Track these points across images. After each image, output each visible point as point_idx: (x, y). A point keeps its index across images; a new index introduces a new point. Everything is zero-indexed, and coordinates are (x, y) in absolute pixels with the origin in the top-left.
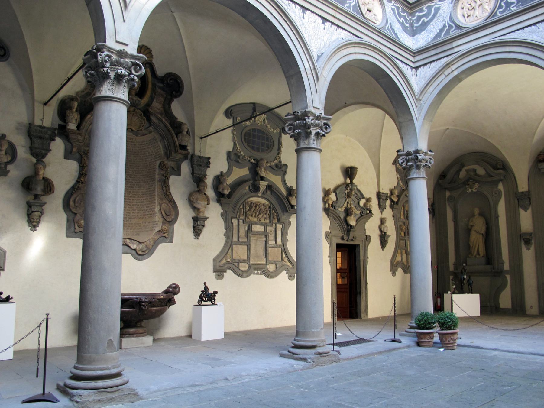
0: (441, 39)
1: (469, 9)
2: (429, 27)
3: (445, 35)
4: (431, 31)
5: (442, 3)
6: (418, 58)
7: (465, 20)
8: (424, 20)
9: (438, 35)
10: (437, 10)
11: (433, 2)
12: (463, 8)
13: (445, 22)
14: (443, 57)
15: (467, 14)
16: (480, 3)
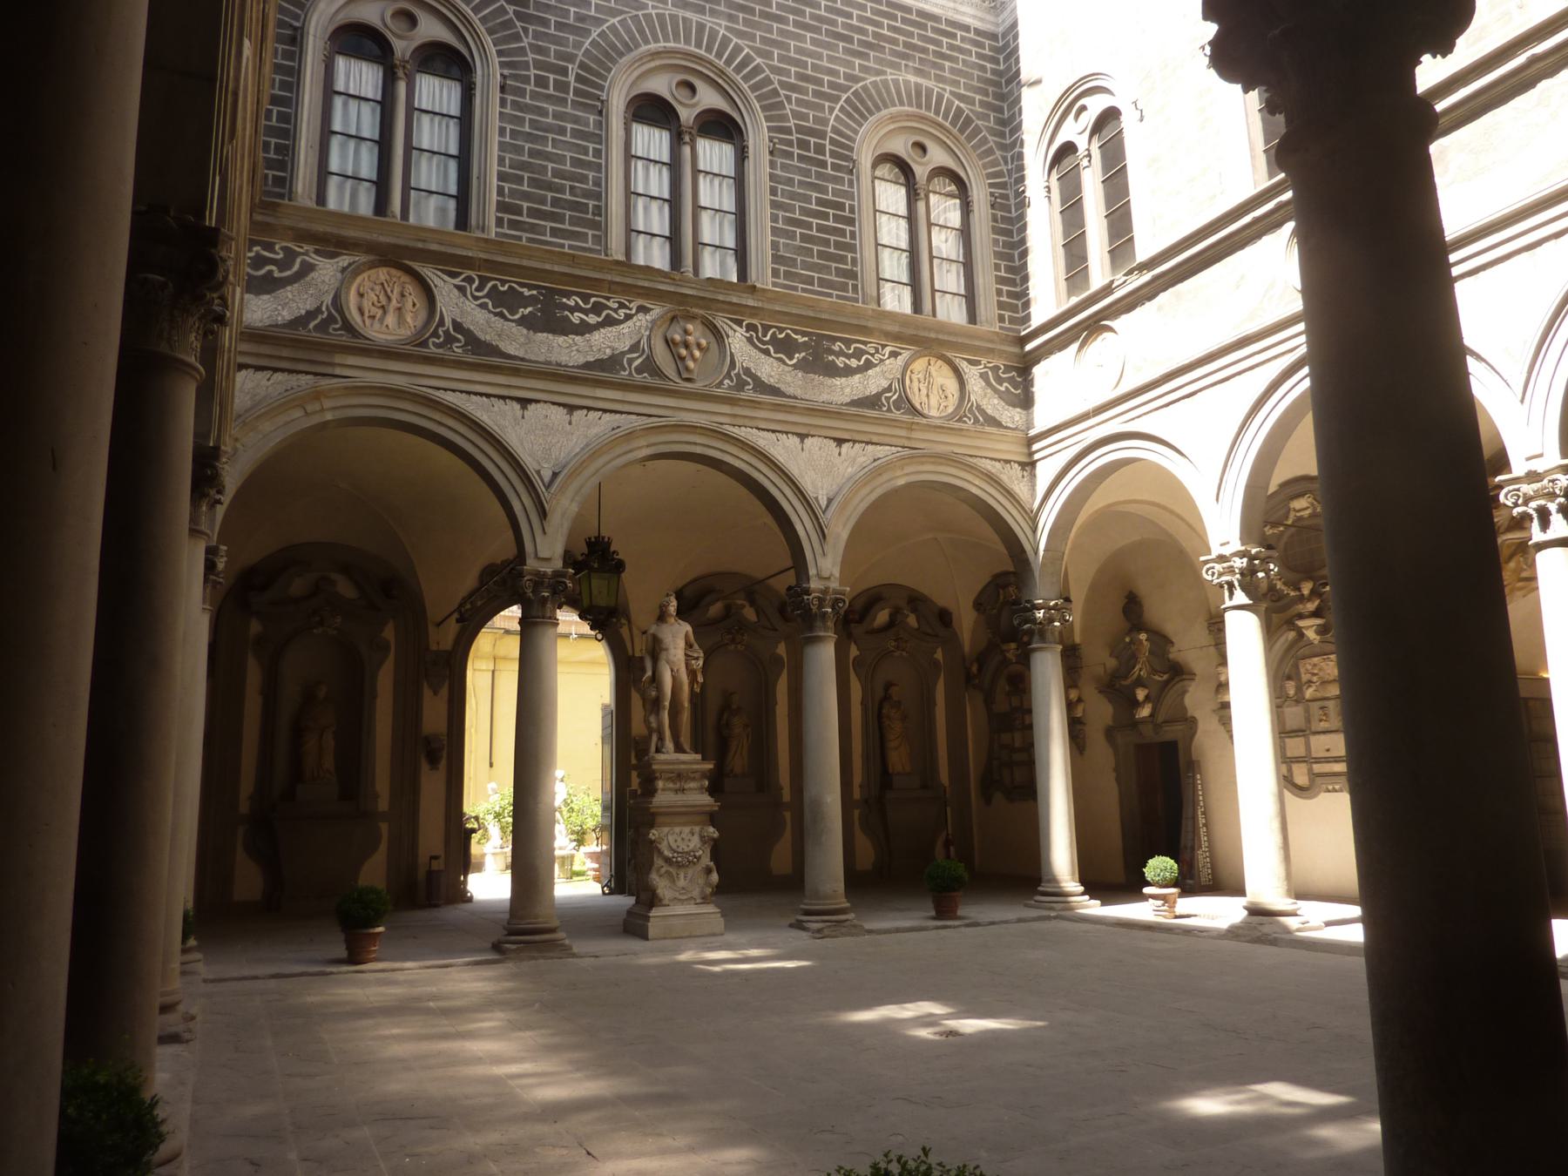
0: (303, 332)
1: (373, 304)
2: (281, 293)
3: (316, 327)
4: (286, 304)
5: (321, 259)
7: (364, 321)
8: (270, 272)
9: (300, 322)
10: (308, 268)
11: (302, 247)
12: (362, 295)
13: (322, 302)
14: (307, 373)
15: (369, 312)
16: (399, 305)
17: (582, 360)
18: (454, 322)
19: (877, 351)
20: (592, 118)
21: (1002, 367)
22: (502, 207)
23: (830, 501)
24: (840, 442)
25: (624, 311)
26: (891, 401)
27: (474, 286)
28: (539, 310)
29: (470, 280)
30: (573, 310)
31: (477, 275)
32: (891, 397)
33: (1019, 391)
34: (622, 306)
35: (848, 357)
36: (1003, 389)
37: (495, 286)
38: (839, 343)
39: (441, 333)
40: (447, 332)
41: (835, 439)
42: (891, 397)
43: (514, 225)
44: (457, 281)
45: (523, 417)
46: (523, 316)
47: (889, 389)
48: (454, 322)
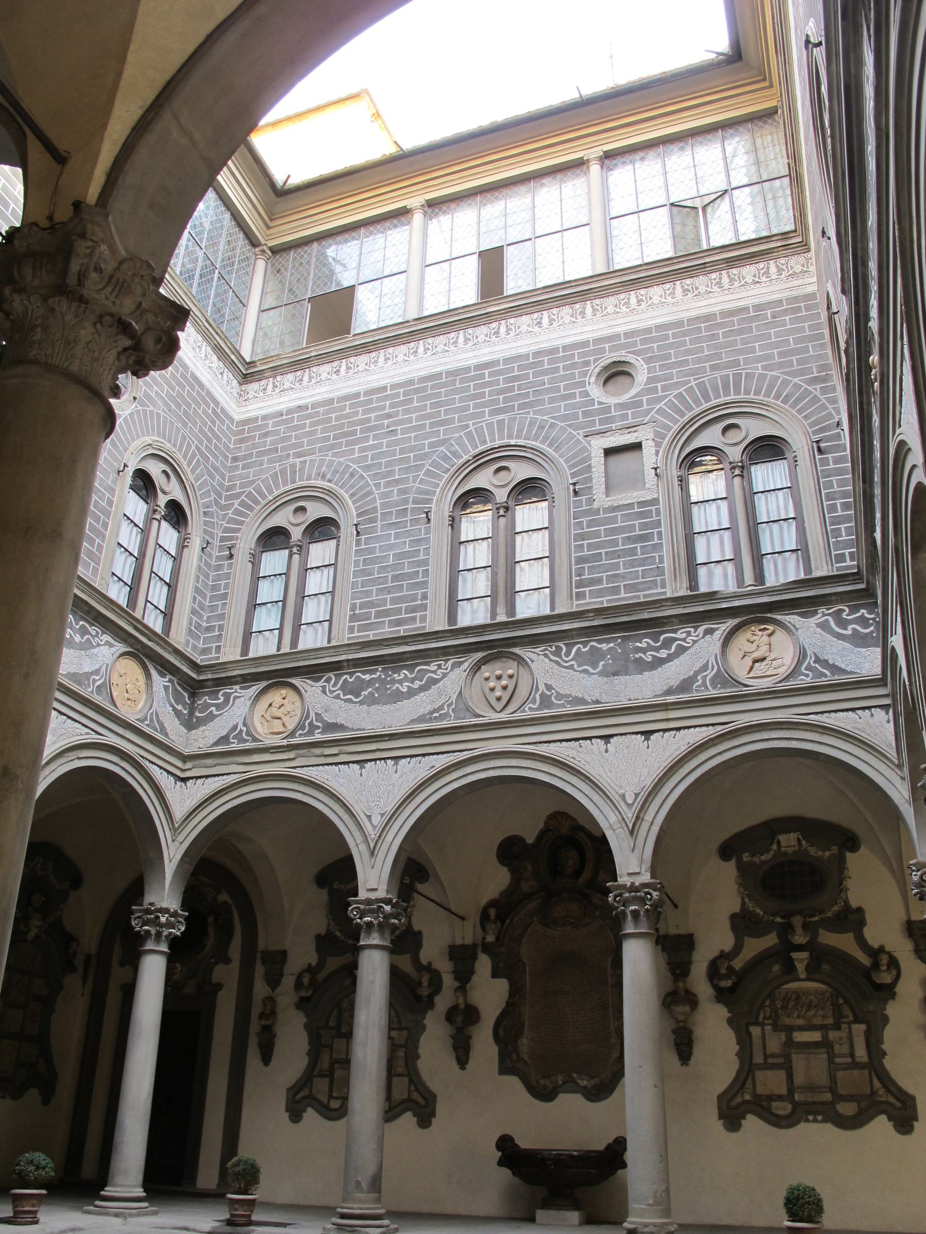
6: (189, 765)
17: (408, 720)
18: (317, 714)
19: (689, 633)
20: (423, 527)
21: (847, 609)
22: (354, 618)
23: (637, 795)
24: (647, 734)
25: (440, 671)
26: (708, 678)
27: (332, 683)
28: (377, 689)
29: (328, 680)
30: (400, 682)
31: (336, 675)
32: (707, 675)
33: (872, 628)
34: (439, 666)
35: (657, 649)
36: (849, 632)
37: (346, 679)
38: (645, 640)
39: (307, 725)
40: (311, 724)
41: (642, 733)
42: (707, 675)
43: (362, 628)
44: (321, 683)
45: (361, 775)
46: (365, 696)
47: (705, 667)
48: (317, 714)
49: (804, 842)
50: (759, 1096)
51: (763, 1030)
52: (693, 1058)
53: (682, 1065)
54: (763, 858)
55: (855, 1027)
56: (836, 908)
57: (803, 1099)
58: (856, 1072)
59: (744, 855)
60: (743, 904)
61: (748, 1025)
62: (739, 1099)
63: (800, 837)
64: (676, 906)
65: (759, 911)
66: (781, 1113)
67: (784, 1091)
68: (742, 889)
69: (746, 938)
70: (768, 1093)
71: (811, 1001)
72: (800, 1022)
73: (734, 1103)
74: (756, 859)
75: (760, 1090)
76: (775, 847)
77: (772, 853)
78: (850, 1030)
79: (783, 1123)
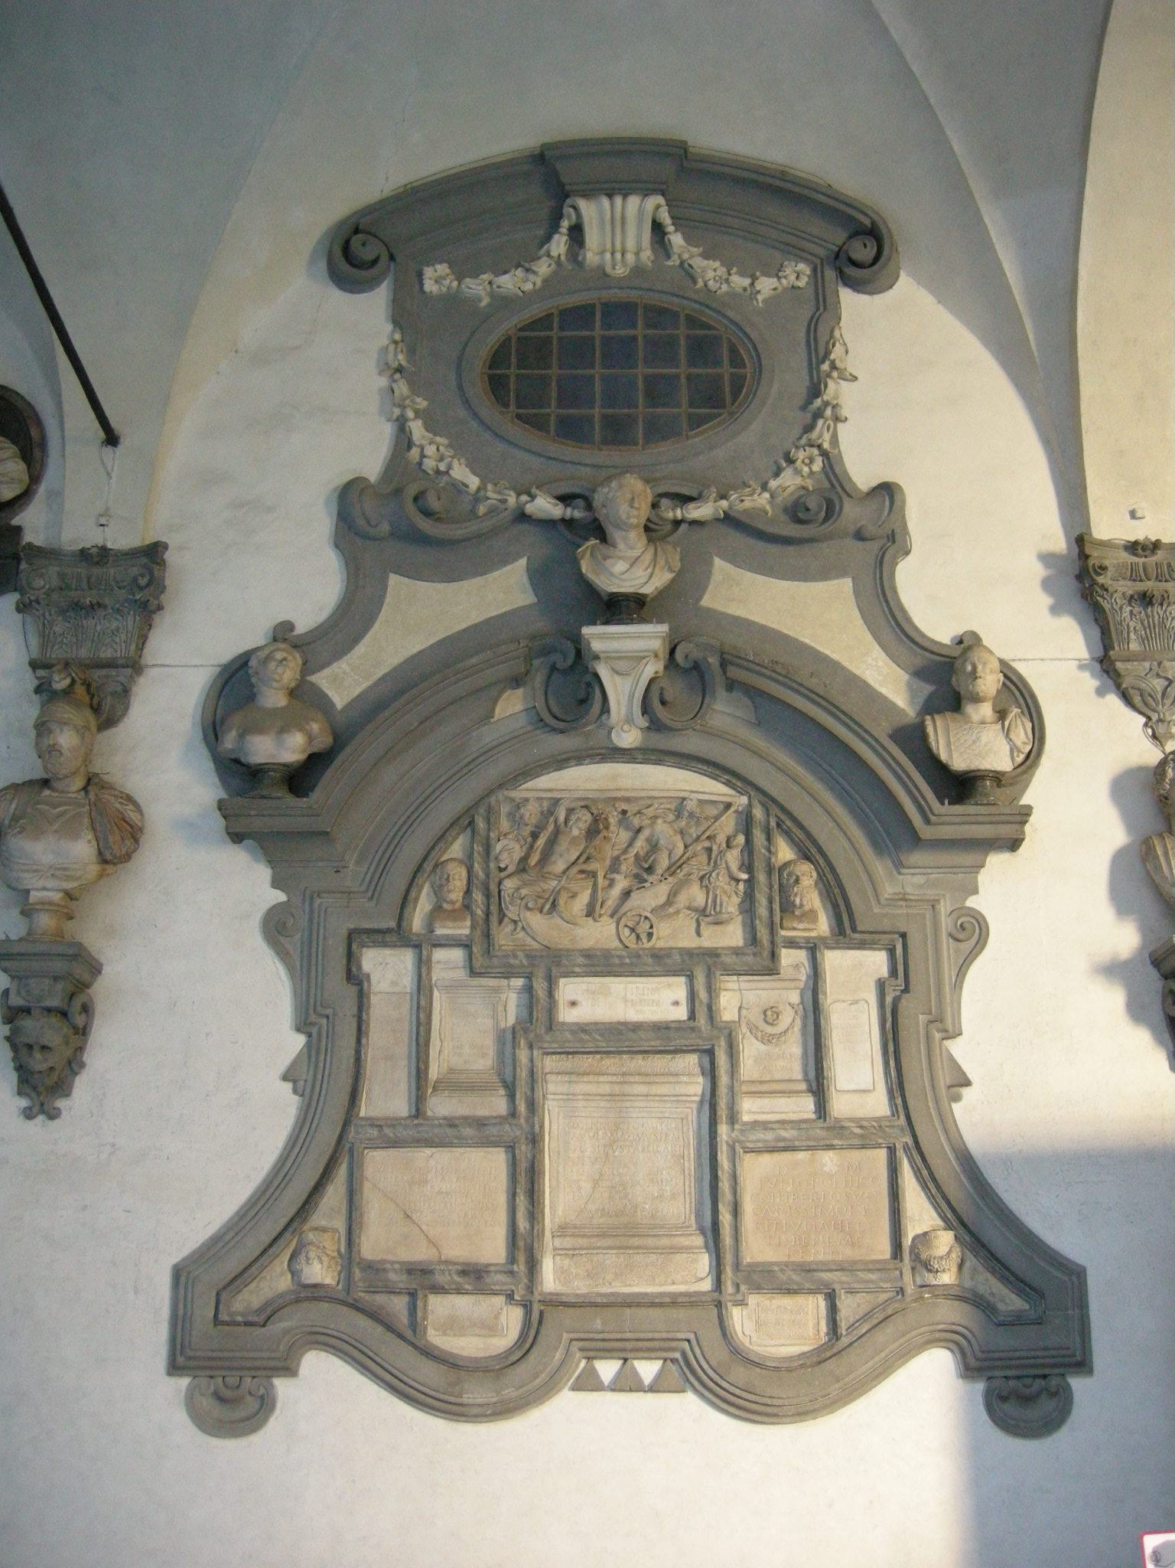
49: (677, 240)
50: (373, 1268)
51: (423, 965)
52: (83, 1087)
53: (28, 1114)
54: (510, 282)
55: (834, 960)
56: (788, 482)
57: (581, 1287)
58: (829, 1160)
59: (429, 272)
60: (403, 440)
61: (357, 940)
62: (276, 1281)
63: (665, 217)
64: (111, 439)
65: (460, 472)
66: (467, 1346)
67: (493, 1248)
68: (402, 388)
69: (394, 579)
70: (420, 1253)
71: (654, 847)
72: (600, 933)
73: (251, 1298)
74: (477, 288)
75: (373, 1244)
76: (559, 245)
77: (543, 268)
78: (816, 974)
79: (476, 1394)
